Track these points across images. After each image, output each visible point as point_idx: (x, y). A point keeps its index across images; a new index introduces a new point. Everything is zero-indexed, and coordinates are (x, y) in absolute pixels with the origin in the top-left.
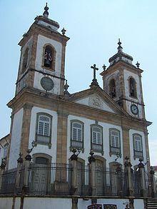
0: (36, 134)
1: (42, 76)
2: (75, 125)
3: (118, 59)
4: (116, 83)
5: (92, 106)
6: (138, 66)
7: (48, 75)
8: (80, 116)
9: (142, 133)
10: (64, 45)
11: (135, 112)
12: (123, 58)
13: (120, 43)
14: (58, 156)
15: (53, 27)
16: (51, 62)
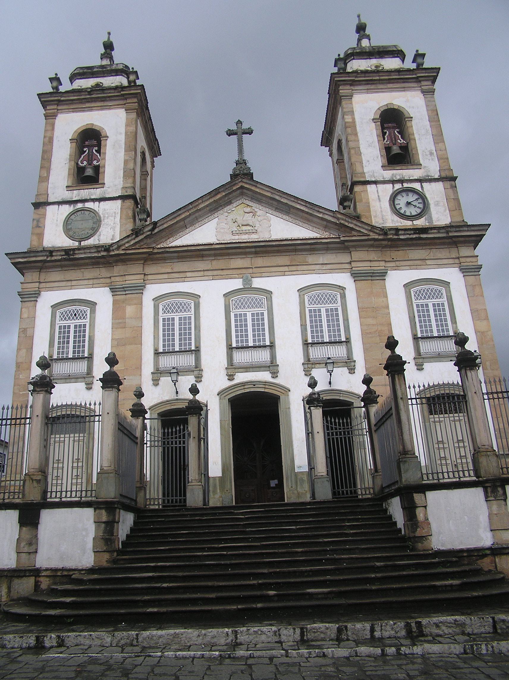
1: (67, 209)
5: (228, 238)
8: (183, 279)
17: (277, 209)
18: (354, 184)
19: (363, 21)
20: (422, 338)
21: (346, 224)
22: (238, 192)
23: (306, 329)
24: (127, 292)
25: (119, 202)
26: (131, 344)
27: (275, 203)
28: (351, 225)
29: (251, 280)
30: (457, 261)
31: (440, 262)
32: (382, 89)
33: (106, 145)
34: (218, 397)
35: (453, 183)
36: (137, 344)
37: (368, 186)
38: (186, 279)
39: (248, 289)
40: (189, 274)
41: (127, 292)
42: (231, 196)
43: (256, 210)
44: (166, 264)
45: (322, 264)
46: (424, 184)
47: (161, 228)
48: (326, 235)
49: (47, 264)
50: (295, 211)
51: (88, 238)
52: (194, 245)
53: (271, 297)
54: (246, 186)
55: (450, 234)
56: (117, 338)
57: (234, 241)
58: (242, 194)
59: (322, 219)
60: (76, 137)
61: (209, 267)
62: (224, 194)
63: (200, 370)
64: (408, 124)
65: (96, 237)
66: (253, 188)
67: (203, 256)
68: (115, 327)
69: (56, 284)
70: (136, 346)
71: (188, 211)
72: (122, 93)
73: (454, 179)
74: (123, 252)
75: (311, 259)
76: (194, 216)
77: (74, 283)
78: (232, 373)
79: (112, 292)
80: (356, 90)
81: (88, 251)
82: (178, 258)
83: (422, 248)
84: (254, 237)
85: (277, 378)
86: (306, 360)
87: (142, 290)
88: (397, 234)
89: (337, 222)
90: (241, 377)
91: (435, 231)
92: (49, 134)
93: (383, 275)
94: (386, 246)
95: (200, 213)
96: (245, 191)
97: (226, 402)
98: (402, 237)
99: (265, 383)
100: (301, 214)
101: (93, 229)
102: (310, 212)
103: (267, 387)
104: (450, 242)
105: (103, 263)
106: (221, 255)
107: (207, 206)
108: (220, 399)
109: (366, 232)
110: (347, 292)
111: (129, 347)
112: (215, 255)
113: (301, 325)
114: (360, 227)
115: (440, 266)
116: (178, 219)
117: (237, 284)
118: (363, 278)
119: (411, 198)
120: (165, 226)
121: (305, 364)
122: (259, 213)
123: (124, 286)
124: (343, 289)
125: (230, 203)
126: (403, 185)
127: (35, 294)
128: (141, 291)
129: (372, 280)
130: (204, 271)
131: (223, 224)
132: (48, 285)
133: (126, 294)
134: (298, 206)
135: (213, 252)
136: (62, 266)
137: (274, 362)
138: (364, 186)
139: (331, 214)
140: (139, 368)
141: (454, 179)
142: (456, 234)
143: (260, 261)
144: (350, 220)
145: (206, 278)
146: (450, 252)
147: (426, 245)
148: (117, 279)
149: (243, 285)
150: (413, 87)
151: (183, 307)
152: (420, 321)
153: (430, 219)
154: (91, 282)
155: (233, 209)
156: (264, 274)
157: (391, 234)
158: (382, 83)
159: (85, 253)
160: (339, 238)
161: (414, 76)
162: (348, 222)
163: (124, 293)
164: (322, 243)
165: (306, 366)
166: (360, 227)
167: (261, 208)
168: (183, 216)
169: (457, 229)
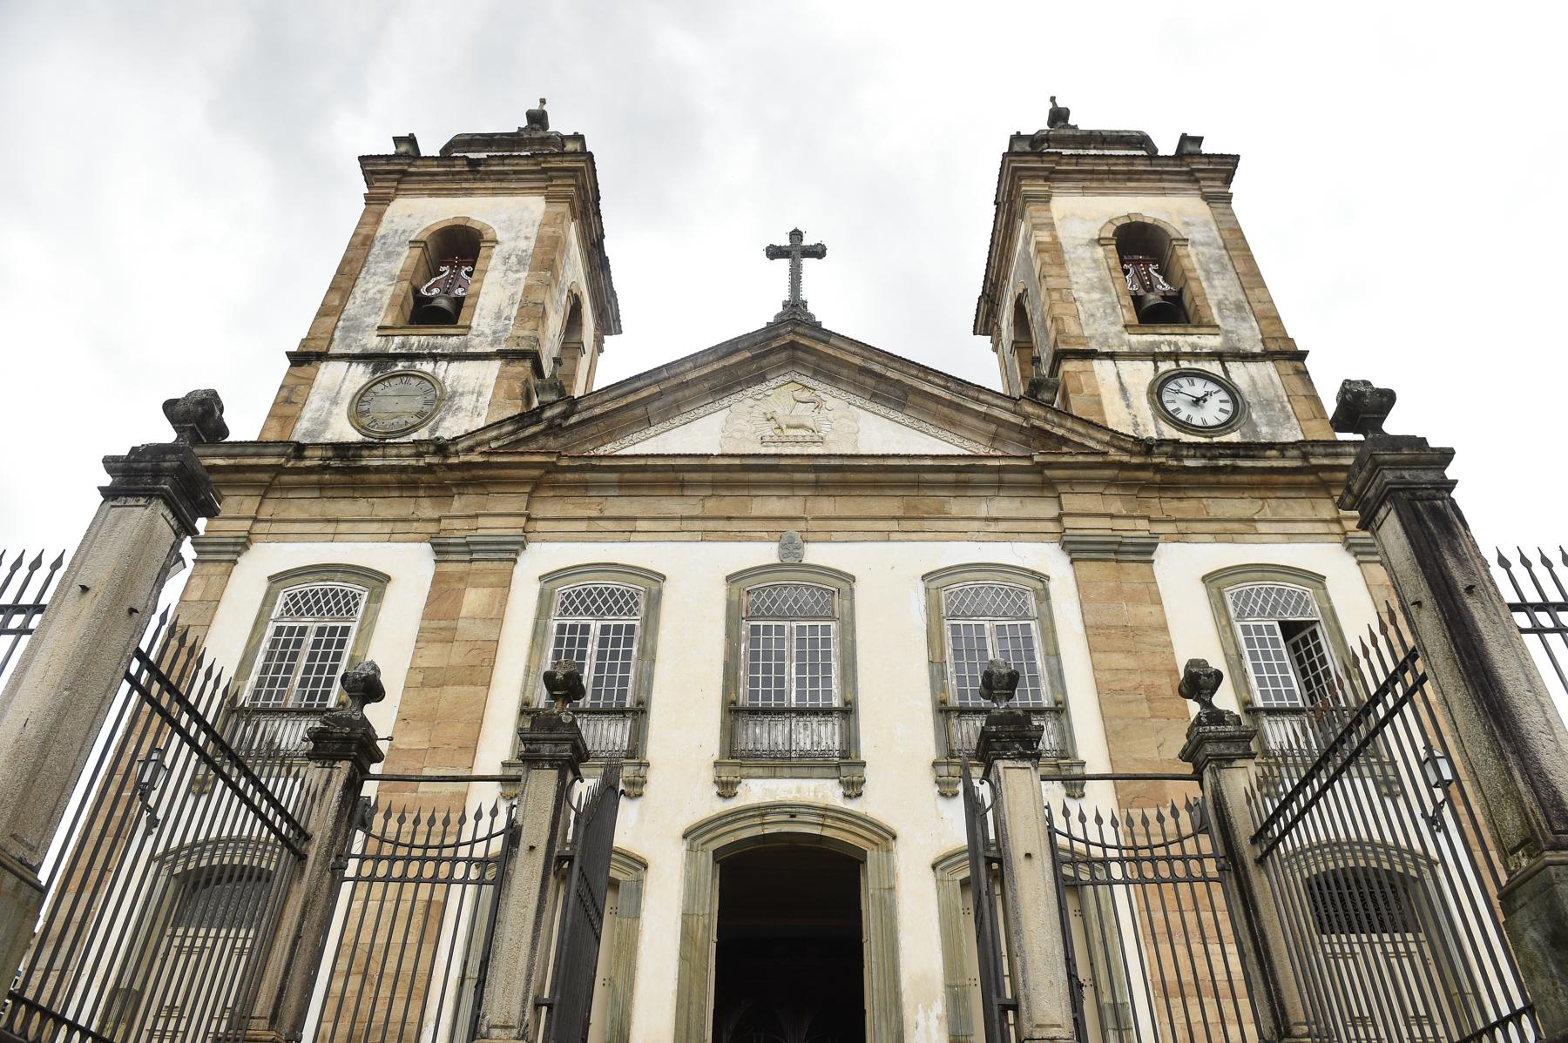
8: (628, 535)
16: (459, 302)
17: (874, 397)
18: (1060, 356)
19: (1060, 105)
20: (1271, 712)
21: (1048, 427)
22: (784, 355)
23: (943, 674)
24: (475, 556)
25: (495, 366)
26: (461, 683)
27: (870, 382)
28: (1060, 432)
30: (1335, 528)
31: (1291, 528)
34: (683, 847)
35: (1299, 364)
36: (476, 685)
37: (1096, 363)
38: (634, 536)
39: (791, 563)
40: (641, 525)
41: (475, 556)
42: (765, 362)
43: (823, 396)
44: (587, 500)
45: (987, 519)
46: (1231, 366)
47: (586, 415)
49: (286, 478)
50: (918, 400)
52: (662, 456)
53: (852, 590)
55: (1314, 461)
58: (793, 362)
59: (986, 417)
60: (424, 239)
61: (697, 512)
63: (641, 764)
64: (1180, 251)
66: (820, 347)
67: (683, 485)
68: (424, 637)
69: (297, 527)
70: (472, 689)
71: (657, 382)
72: (543, 165)
73: (1302, 356)
74: (480, 459)
75: (956, 507)
76: (671, 398)
77: (343, 527)
78: (731, 779)
79: (437, 553)
80: (1058, 188)
81: (394, 452)
82: (621, 485)
83: (1241, 495)
85: (860, 800)
86: (945, 753)
87: (517, 552)
88: (1179, 458)
89: (1024, 424)
90: (757, 791)
91: (1274, 453)
92: (365, 231)
93: (1145, 551)
94: (1147, 486)
95: (687, 392)
96: (800, 354)
97: (706, 860)
99: (825, 812)
100: (932, 406)
101: (420, 414)
102: (957, 400)
103: (829, 822)
104: (1311, 483)
105: (429, 487)
106: (730, 485)
107: (705, 378)
108: (690, 849)
109: (1098, 447)
110: (1053, 586)
111: (451, 692)
112: (714, 485)
113: (931, 662)
114: (1080, 435)
115: (1290, 537)
116: (631, 398)
117: (764, 553)
118: (1093, 555)
119: (1199, 387)
120: (597, 411)
121: (941, 764)
122: (831, 402)
123: (468, 539)
124: (1043, 578)
125: (761, 378)
126: (1178, 365)
128: (513, 556)
129: (1117, 561)
130: (682, 518)
131: (740, 421)
132: (275, 528)
133: (471, 561)
134: (927, 388)
135: (708, 476)
136: (321, 486)
137: (853, 755)
138: (1087, 363)
139: (1009, 405)
141: (1302, 356)
142: (1326, 461)
143: (826, 506)
144: (1056, 420)
145: (687, 536)
146: (1313, 508)
147: (1251, 487)
148: (457, 524)
149: (782, 556)
150: (1185, 189)
151: (616, 602)
152: (1257, 668)
154: (387, 528)
155: (767, 393)
157: (1160, 455)
158: (1115, 180)
159: (384, 456)
160: (1030, 457)
161: (1184, 169)
162: (1055, 425)
164: (985, 469)
165: (943, 770)
166: (1080, 435)
167: (835, 392)
168: (644, 394)
169: (1330, 450)
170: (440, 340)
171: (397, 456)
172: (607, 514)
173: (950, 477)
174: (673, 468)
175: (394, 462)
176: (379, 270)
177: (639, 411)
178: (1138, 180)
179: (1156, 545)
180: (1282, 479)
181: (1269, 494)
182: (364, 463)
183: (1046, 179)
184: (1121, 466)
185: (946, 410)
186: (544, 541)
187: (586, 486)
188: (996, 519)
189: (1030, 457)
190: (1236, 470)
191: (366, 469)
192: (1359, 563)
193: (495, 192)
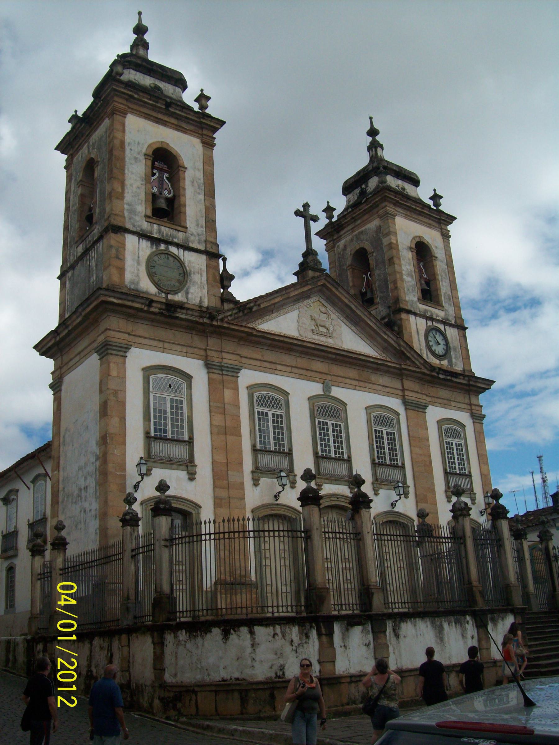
0: (147, 436)
2: (265, 401)
3: (373, 183)
4: (372, 262)
5: (309, 337)
6: (437, 205)
7: (168, 243)
8: (273, 371)
9: (464, 417)
10: (209, 144)
11: (440, 349)
12: (392, 182)
13: (373, 132)
14: (218, 503)
15: (168, 89)
16: (171, 202)
17: (348, 317)
21: (406, 352)
22: (319, 288)
24: (224, 372)
27: (348, 311)
29: (330, 388)
32: (416, 219)
33: (184, 179)
39: (326, 395)
40: (279, 367)
41: (224, 372)
46: (447, 328)
48: (383, 357)
49: (141, 314)
51: (175, 293)
54: (328, 285)
55: (471, 383)
56: (217, 424)
57: (314, 341)
58: (320, 291)
61: (294, 364)
62: (310, 287)
65: (183, 292)
66: (334, 290)
74: (226, 325)
75: (374, 378)
77: (167, 345)
81: (190, 313)
82: (270, 345)
84: (330, 342)
91: (462, 377)
93: (425, 407)
96: (324, 289)
98: (441, 376)
100: (368, 329)
102: (378, 331)
106: (307, 354)
109: (419, 365)
112: (302, 353)
114: (415, 358)
122: (333, 316)
125: (308, 297)
127: (126, 348)
130: (292, 367)
134: (369, 322)
135: (301, 349)
136: (153, 321)
140: (241, 464)
143: (337, 369)
144: (409, 350)
145: (294, 375)
153: (450, 362)
154: (185, 349)
156: (340, 384)
160: (400, 365)
162: (408, 351)
163: (221, 373)
164: (387, 366)
165: (375, 486)
166: (415, 358)
167: (334, 311)
168: (277, 300)
170: (175, 233)
171: (192, 315)
172: (266, 358)
173: (375, 366)
174: (291, 344)
175: (190, 318)
176: (134, 171)
177: (273, 307)
178: (422, 216)
179: (427, 406)
180: (460, 386)
181: (455, 390)
182: (177, 315)
183: (394, 204)
184: (424, 374)
185: (372, 333)
186: (245, 368)
187: (258, 343)
188: (386, 387)
189: (400, 365)
190: (450, 381)
191: (177, 318)
192: (474, 422)
193: (178, 128)
